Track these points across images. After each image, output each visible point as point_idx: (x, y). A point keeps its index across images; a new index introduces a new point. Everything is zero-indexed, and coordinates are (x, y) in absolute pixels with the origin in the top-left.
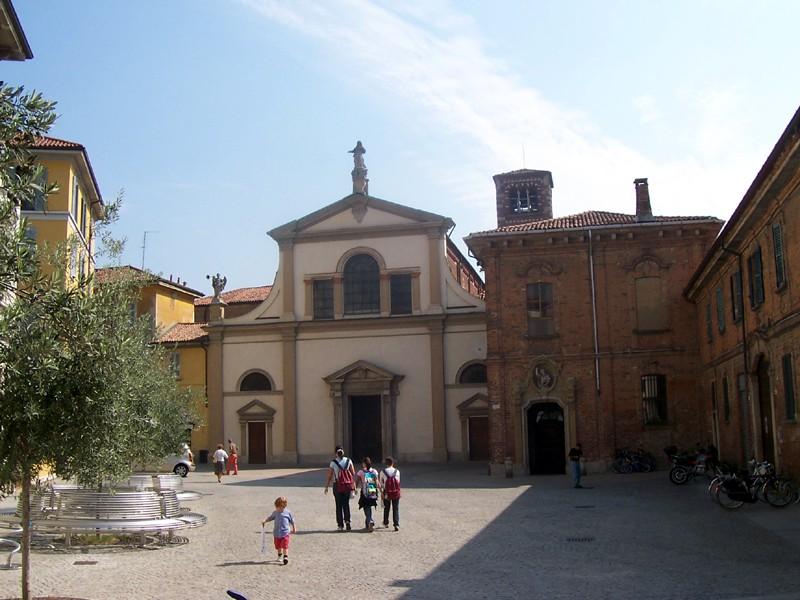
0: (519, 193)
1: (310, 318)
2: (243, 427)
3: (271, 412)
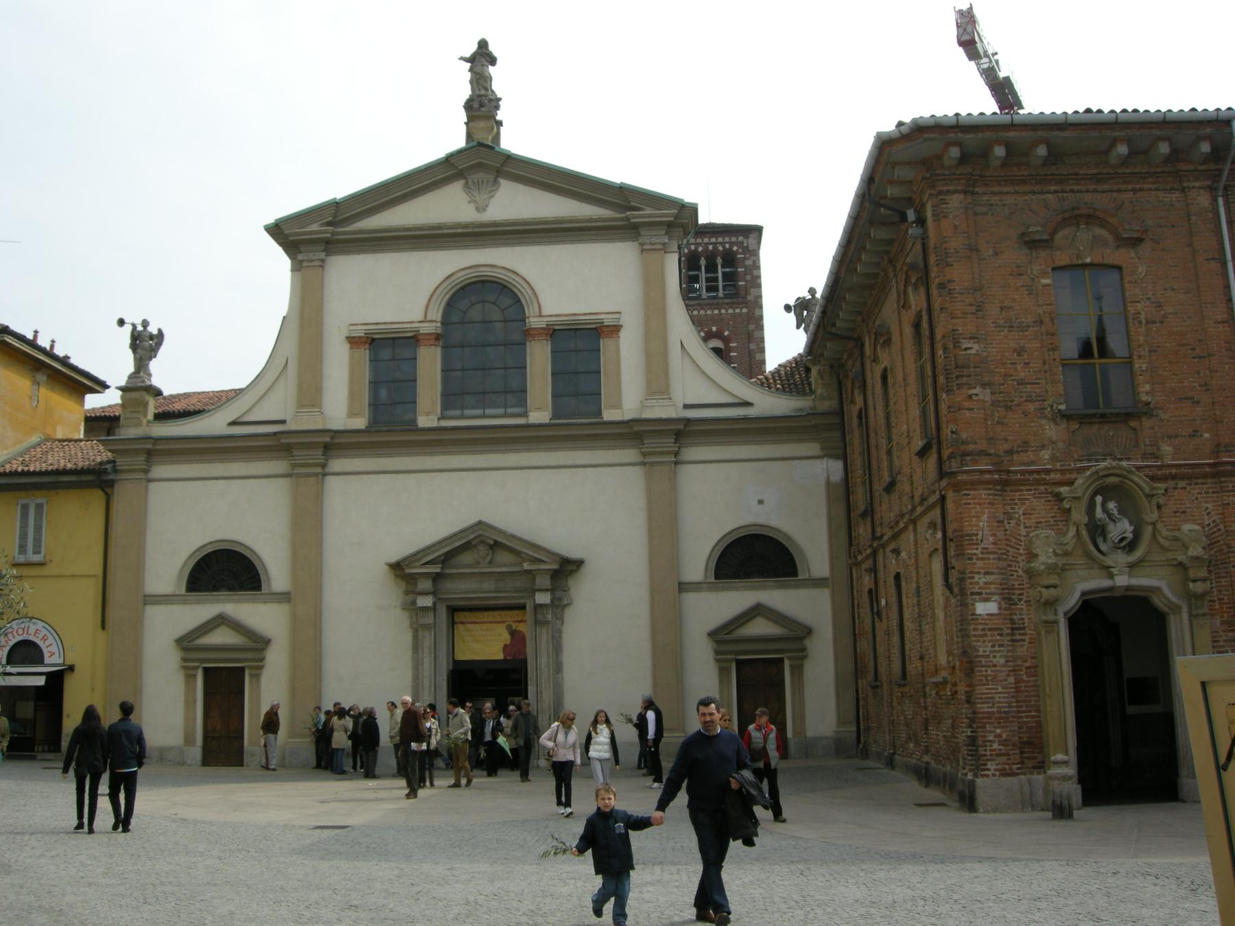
0: (703, 262)
1: (360, 423)
2: (190, 678)
3: (259, 643)
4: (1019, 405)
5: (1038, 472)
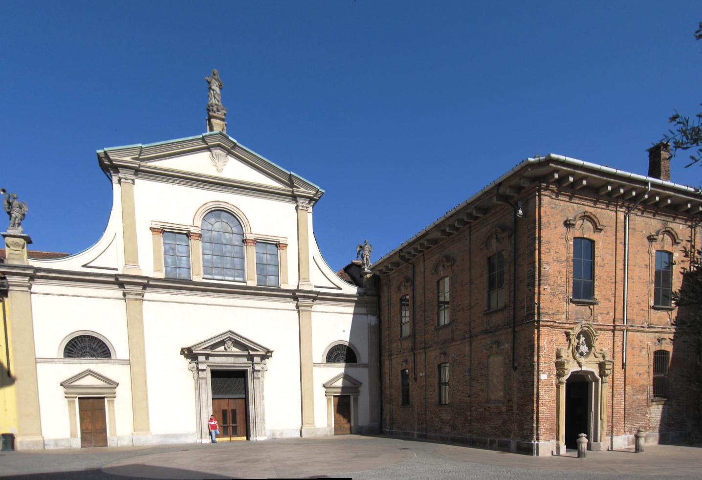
2: (71, 403)
3: (113, 385)
4: (557, 295)
5: (561, 323)
